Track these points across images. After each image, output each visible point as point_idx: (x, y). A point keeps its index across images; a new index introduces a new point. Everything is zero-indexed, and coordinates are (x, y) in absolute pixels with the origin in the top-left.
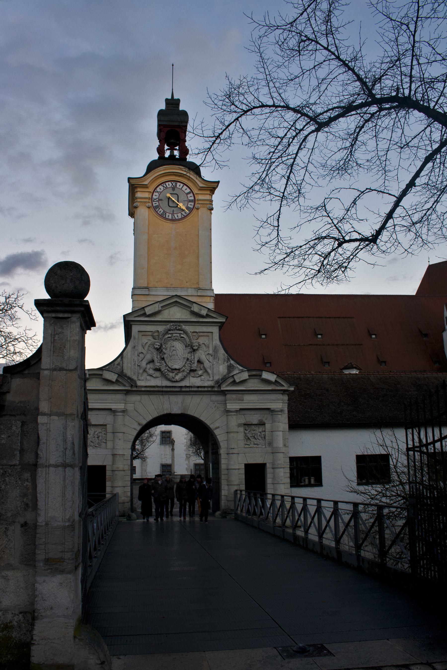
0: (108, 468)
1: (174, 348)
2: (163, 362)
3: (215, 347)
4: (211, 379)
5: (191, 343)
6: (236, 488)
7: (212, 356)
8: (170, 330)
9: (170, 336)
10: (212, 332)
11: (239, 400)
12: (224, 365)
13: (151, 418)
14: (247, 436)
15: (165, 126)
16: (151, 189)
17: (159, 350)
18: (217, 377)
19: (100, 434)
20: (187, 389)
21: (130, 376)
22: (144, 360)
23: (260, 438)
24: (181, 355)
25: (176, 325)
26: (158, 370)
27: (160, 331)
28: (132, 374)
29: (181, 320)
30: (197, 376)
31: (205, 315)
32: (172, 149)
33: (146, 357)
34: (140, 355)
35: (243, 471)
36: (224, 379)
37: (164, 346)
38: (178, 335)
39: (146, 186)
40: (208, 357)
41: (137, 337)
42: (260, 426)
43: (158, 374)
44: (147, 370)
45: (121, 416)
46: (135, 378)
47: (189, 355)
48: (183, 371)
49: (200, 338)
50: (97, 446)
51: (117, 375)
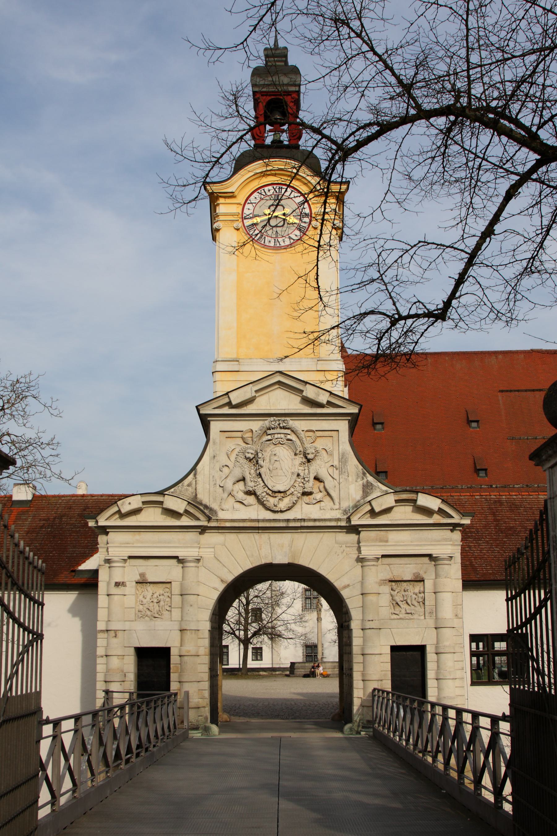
0: (173, 652)
1: (276, 458)
3: (343, 455)
4: (337, 506)
5: (305, 449)
6: (376, 685)
7: (337, 469)
8: (269, 429)
9: (269, 437)
11: (381, 541)
12: (357, 484)
13: (241, 571)
15: (263, 94)
16: (241, 199)
19: (162, 597)
20: (298, 524)
21: (208, 504)
22: (229, 478)
23: (416, 604)
28: (211, 499)
29: (287, 412)
30: (315, 502)
32: (277, 131)
33: (233, 472)
35: (388, 658)
36: (357, 507)
38: (282, 436)
39: (232, 195)
40: (331, 470)
41: (218, 441)
42: (416, 583)
43: (251, 499)
44: (234, 493)
45: (194, 568)
46: (215, 506)
47: (302, 468)
50: (157, 616)
51: (186, 503)
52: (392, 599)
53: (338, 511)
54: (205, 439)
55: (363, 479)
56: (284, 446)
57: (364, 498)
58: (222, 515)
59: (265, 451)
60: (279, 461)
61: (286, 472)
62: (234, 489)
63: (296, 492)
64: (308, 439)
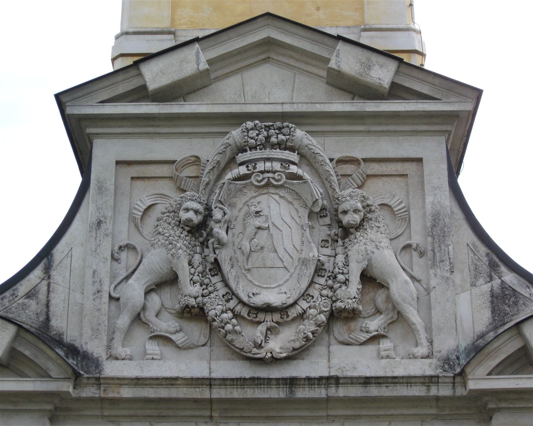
1: (258, 222)
2: (215, 280)
3: (436, 218)
4: (422, 350)
5: (336, 200)
7: (422, 254)
9: (243, 170)
10: (419, 160)
12: (475, 290)
17: (199, 231)
18: (446, 344)
20: (320, 393)
21: (77, 344)
22: (134, 276)
24: (290, 248)
25: (268, 128)
26: (194, 313)
27: (203, 158)
28: (87, 331)
29: (288, 108)
30: (364, 337)
31: (386, 83)
33: (144, 261)
34: (123, 255)
36: (477, 350)
37: (217, 214)
38: (277, 166)
40: (405, 258)
44: (150, 315)
46: (95, 347)
48: (302, 316)
49: (371, 184)
51: (12, 330)
53: (428, 361)
54: (78, 179)
55: (491, 279)
56: (282, 192)
57: (496, 328)
58: (111, 369)
59: (232, 206)
60: (268, 228)
61: (286, 258)
62: (149, 305)
63: (312, 311)
64: (343, 180)
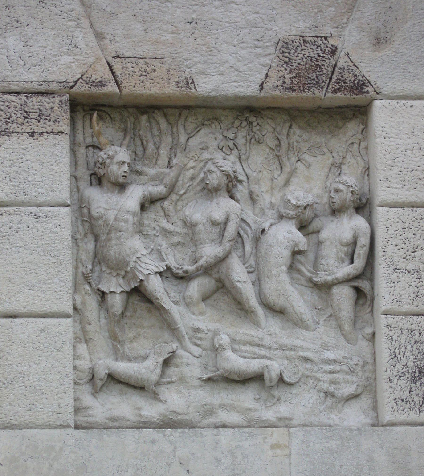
14: (121, 268)
23: (299, 301)
52: (99, 258)
